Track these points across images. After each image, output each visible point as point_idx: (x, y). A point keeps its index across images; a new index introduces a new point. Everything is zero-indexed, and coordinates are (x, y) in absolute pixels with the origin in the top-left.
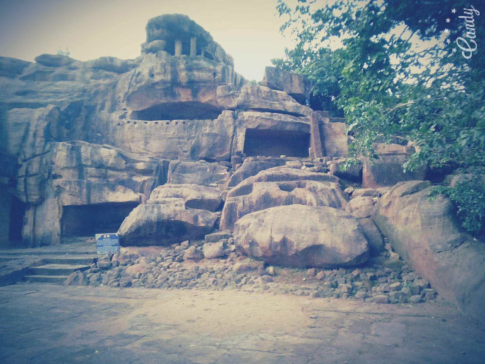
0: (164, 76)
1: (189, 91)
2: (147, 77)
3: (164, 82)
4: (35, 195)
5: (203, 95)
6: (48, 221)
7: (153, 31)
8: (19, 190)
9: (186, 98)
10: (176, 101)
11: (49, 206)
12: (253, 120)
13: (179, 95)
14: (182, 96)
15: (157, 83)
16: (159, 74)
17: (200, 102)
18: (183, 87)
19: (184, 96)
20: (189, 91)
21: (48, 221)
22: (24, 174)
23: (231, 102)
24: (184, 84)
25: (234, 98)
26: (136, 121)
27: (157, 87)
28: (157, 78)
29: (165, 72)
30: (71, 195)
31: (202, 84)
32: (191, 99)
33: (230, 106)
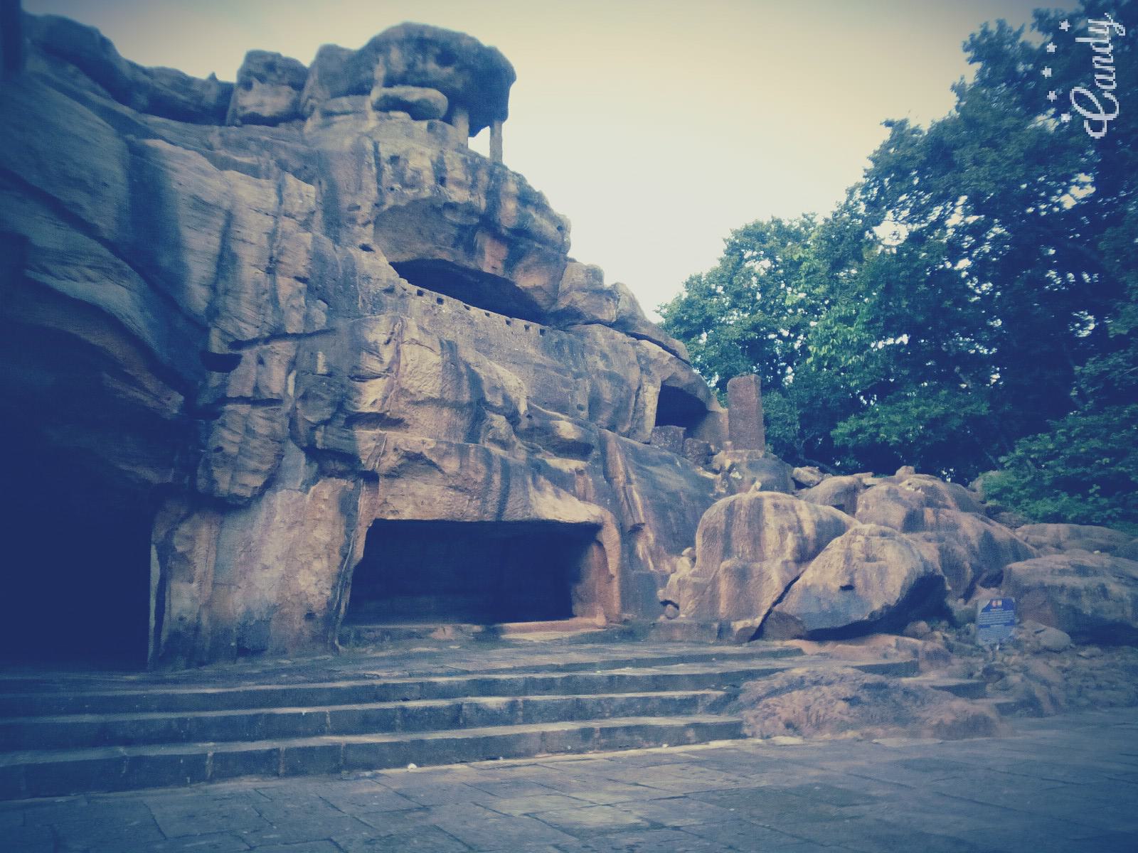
0: (472, 195)
1: (503, 252)
2: (428, 178)
3: (470, 210)
4: (256, 471)
5: (527, 269)
6: (265, 567)
7: (425, 61)
8: (220, 449)
9: (492, 264)
10: (472, 265)
11: (278, 518)
12: (665, 363)
13: (482, 252)
14: (487, 258)
15: (452, 207)
16: (459, 184)
17: (513, 284)
18: (497, 236)
19: (490, 259)
20: (503, 252)
21: (265, 567)
22: (248, 393)
23: (601, 308)
24: (504, 231)
25: (608, 300)
26: (444, 297)
27: (449, 216)
28: (458, 195)
29: (473, 186)
30: (456, 488)
31: (536, 245)
32: (500, 272)
33: (600, 317)
